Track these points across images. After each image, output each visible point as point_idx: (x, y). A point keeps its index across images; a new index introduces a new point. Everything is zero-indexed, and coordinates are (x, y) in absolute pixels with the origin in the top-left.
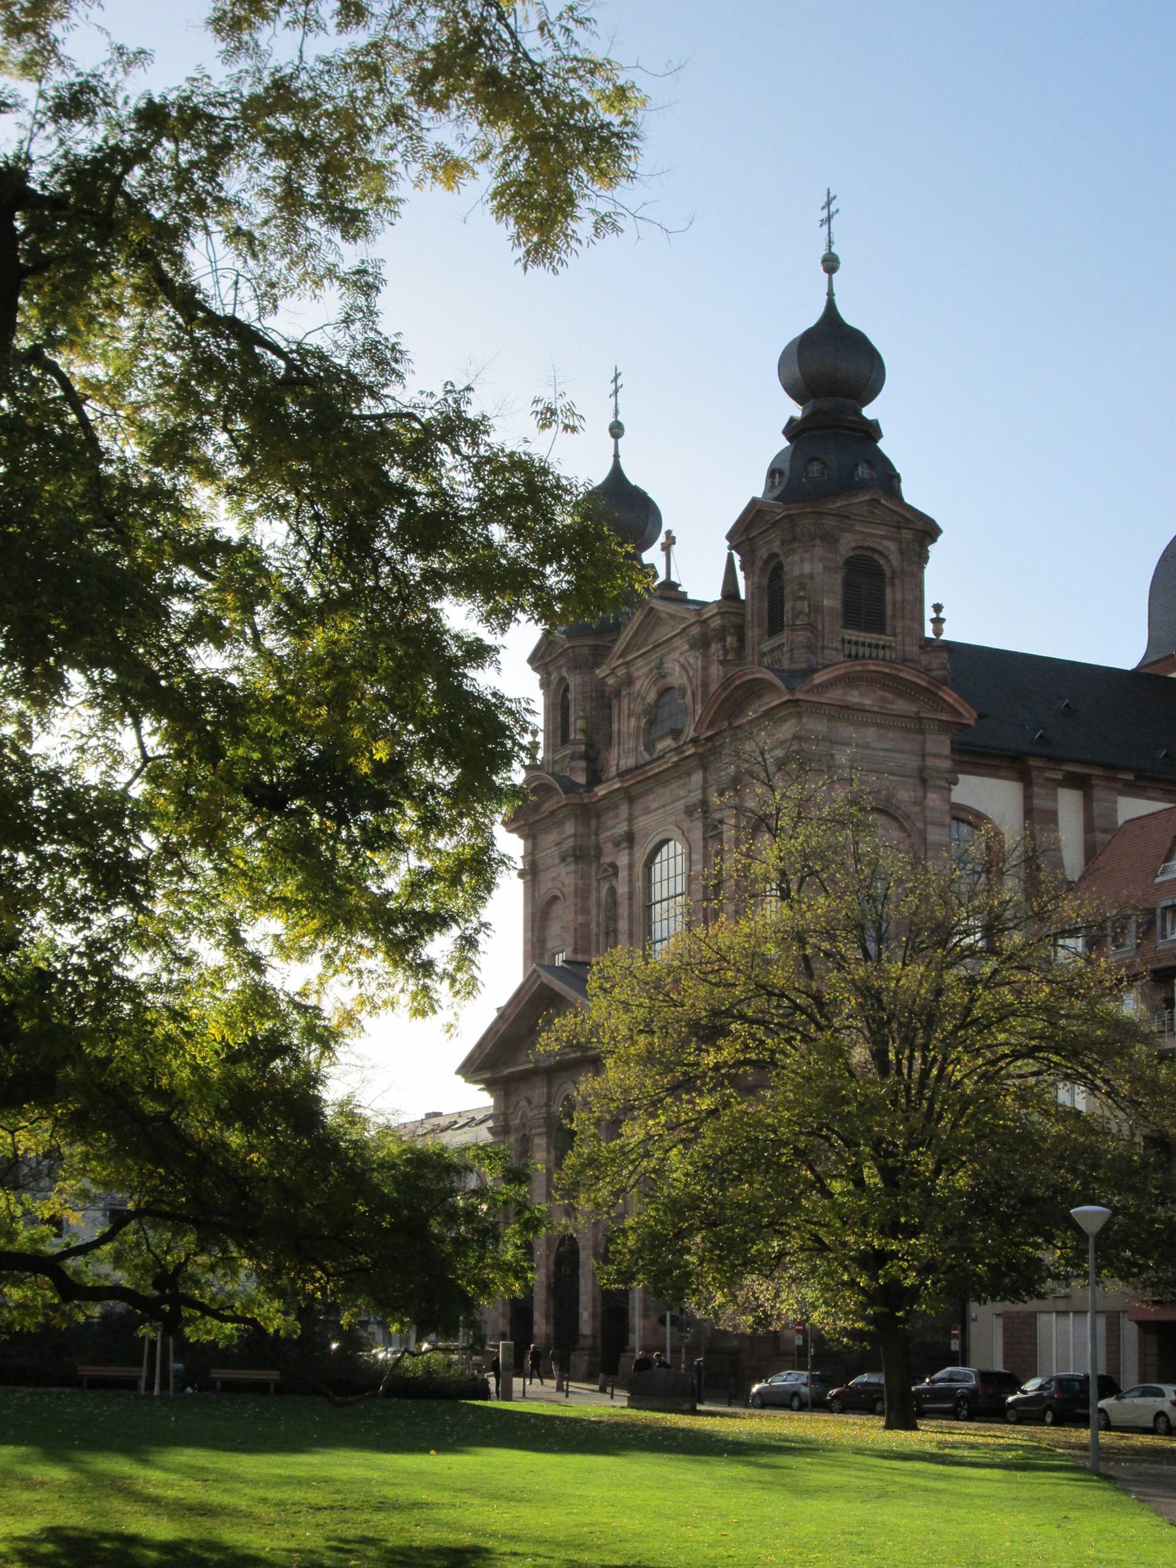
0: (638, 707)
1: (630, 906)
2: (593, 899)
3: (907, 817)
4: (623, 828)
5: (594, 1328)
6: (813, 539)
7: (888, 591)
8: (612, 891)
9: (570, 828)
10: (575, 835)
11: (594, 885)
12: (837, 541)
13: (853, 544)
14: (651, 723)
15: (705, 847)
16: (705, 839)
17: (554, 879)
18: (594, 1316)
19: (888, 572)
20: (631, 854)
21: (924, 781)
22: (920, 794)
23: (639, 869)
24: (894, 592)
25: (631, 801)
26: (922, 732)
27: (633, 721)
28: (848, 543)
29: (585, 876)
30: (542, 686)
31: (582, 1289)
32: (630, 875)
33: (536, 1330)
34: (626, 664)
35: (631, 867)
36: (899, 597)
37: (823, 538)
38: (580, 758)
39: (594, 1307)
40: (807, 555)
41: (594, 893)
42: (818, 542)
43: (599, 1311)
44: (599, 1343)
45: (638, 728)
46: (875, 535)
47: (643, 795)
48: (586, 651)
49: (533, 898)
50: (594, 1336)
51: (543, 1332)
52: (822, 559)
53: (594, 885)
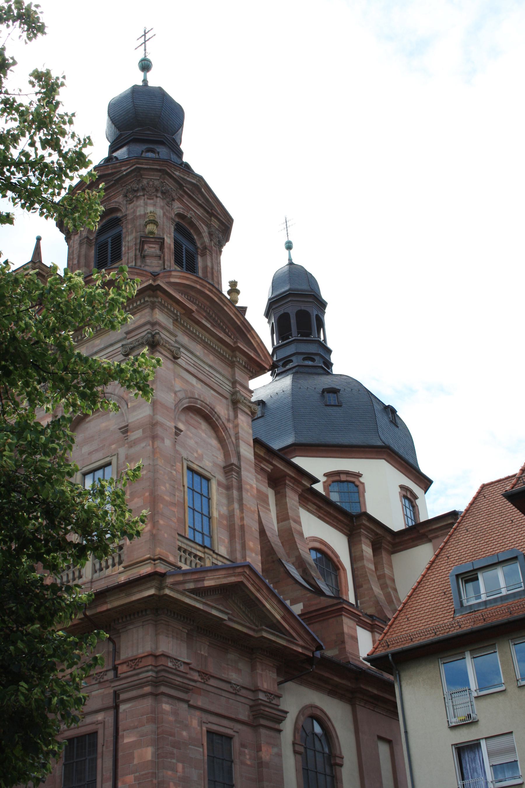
3: (225, 429)
6: (157, 191)
7: (200, 259)
13: (181, 211)
22: (231, 413)
24: (205, 261)
26: (232, 365)
37: (163, 193)
40: (150, 202)
42: (159, 194)
52: (162, 208)
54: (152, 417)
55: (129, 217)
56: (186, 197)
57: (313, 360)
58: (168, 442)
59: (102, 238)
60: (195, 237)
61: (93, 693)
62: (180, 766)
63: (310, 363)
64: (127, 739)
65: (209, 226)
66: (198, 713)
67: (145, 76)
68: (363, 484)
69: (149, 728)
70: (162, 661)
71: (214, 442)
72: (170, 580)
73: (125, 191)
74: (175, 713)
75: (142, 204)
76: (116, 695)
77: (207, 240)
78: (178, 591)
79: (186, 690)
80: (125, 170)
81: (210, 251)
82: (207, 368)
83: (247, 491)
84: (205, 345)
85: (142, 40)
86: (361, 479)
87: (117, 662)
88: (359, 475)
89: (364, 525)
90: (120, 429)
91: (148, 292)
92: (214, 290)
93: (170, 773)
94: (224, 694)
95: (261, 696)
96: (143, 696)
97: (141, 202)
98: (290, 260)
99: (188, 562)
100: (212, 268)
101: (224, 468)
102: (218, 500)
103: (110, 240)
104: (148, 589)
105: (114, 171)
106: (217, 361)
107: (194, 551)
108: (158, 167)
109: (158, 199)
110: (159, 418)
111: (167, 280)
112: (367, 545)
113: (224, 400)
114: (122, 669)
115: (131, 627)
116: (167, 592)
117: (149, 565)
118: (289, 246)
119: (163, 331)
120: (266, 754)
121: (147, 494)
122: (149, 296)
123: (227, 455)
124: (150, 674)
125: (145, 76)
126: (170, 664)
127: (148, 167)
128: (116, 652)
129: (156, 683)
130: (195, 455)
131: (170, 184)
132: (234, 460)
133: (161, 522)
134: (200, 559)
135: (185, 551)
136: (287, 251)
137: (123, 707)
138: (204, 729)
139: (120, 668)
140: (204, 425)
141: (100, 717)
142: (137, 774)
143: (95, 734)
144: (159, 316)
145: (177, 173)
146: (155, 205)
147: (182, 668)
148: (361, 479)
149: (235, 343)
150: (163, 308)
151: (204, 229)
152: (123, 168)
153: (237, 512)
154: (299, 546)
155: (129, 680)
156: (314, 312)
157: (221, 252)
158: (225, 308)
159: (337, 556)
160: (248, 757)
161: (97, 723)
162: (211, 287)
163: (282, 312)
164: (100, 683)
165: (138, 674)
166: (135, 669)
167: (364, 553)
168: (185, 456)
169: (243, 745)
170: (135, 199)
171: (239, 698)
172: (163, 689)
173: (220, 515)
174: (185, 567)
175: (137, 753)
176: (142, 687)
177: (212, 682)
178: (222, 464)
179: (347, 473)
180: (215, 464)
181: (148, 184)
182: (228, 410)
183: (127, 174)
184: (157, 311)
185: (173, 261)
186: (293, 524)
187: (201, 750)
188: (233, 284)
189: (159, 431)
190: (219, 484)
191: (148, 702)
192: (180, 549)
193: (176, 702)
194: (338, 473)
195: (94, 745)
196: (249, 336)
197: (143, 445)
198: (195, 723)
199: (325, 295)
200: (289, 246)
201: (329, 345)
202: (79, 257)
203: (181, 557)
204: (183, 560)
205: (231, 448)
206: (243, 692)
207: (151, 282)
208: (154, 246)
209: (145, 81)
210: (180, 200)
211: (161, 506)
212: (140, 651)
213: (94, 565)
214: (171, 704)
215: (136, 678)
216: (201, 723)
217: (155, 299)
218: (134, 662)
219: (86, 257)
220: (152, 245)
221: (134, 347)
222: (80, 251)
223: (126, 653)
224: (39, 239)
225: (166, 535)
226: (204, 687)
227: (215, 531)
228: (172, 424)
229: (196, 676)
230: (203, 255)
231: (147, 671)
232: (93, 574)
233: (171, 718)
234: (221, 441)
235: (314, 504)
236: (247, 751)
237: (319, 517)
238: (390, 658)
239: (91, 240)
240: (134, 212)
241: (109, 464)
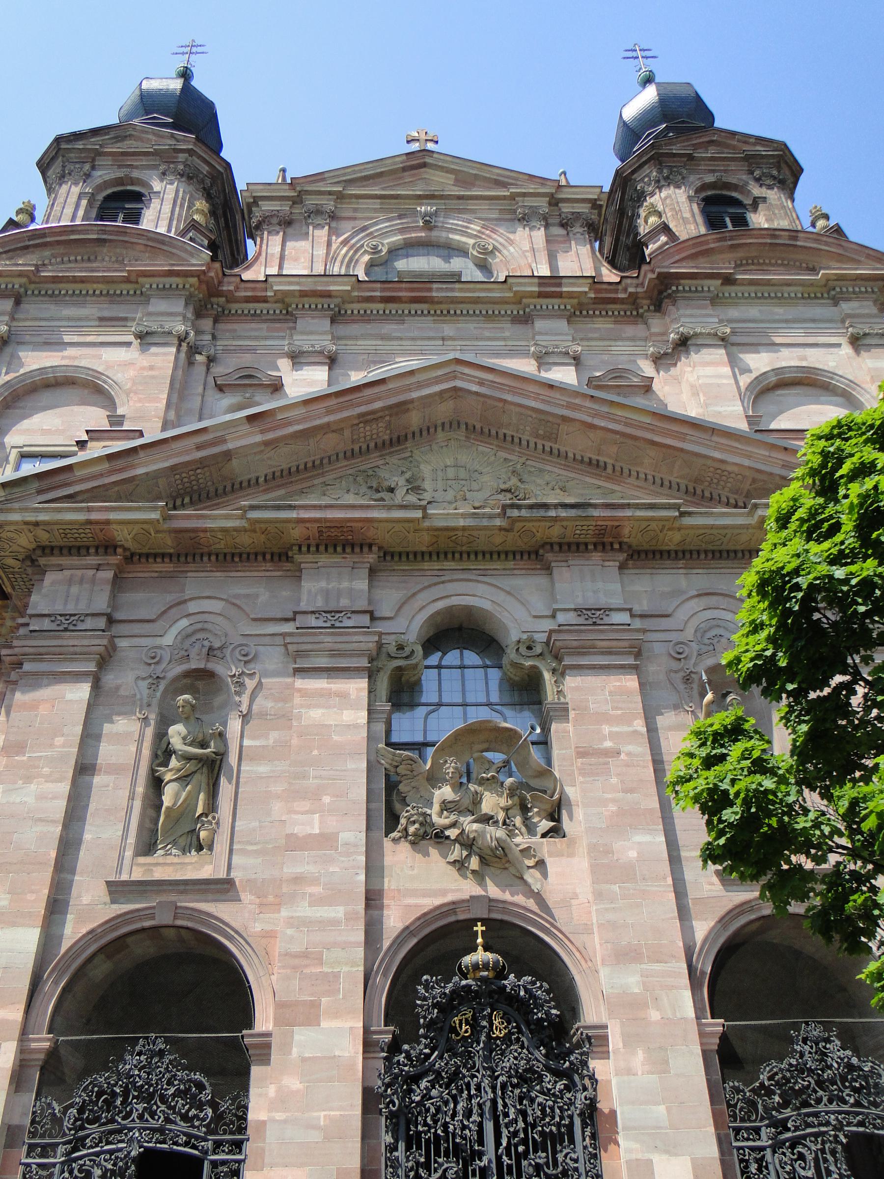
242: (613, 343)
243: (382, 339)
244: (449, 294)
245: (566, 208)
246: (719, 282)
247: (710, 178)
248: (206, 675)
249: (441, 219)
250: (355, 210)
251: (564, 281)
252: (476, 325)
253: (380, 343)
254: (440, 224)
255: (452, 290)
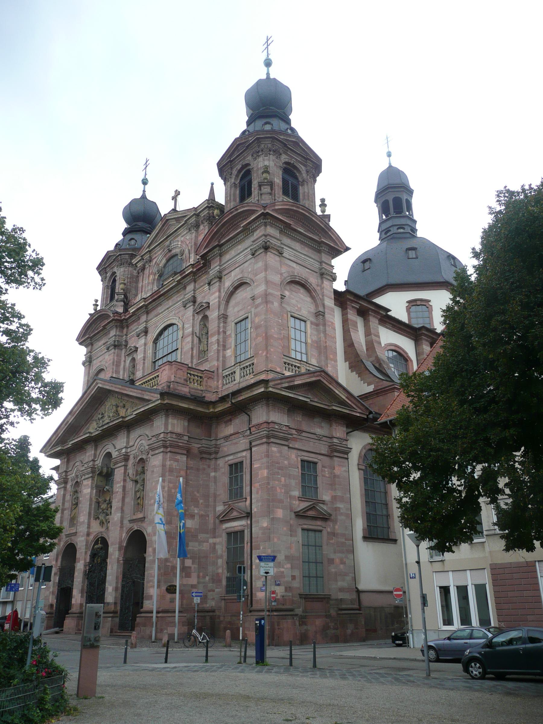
0: (155, 270)
1: (144, 363)
2: (122, 366)
3: (315, 291)
4: (142, 327)
5: (116, 598)
6: (270, 151)
7: (300, 187)
8: (133, 360)
9: (113, 333)
10: (115, 335)
11: (123, 359)
12: (281, 154)
13: (287, 160)
14: (160, 276)
15: (193, 320)
16: (193, 316)
17: (100, 362)
18: (116, 589)
19: (300, 179)
20: (146, 338)
21: (322, 275)
22: (320, 281)
23: (150, 345)
25: (148, 313)
26: (319, 251)
27: (151, 277)
28: (284, 158)
29: (119, 356)
30: (102, 281)
31: (109, 571)
32: (145, 348)
33: (73, 601)
34: (150, 251)
35: (145, 344)
36: (306, 190)
37: (274, 151)
38: (121, 301)
39: (117, 583)
41: (122, 363)
43: (120, 585)
44: (119, 608)
45: (154, 279)
46: (296, 160)
47: (154, 309)
48: (127, 256)
49: (89, 373)
50: (115, 603)
51: (79, 602)
52: (273, 161)
53: (123, 359)
54: (266, 290)
55: (255, 169)
56: (289, 150)
57: (404, 228)
58: (276, 304)
59: (243, 183)
60: (298, 174)
61: (241, 442)
62: (283, 479)
63: (402, 231)
64: (256, 466)
65: (305, 166)
66: (295, 451)
67: (268, 70)
68: (431, 306)
69: (265, 460)
70: (271, 425)
71: (309, 299)
72: (271, 384)
73: (252, 153)
74: (280, 452)
75: (262, 160)
76: (251, 443)
77: (304, 175)
78: (277, 389)
79: (286, 439)
80: (251, 140)
81: (307, 182)
82: (303, 256)
83: (329, 326)
84: (302, 243)
85: (266, 46)
86: (430, 303)
87: (250, 426)
88: (429, 301)
89: (424, 334)
90: (251, 298)
91: (262, 217)
92: (305, 209)
93: (277, 482)
94: (312, 440)
95: (335, 440)
96: (262, 444)
97: (261, 159)
98: (390, 164)
99: (291, 370)
100: (308, 193)
101: (316, 313)
102: (311, 333)
103: (246, 183)
104: (260, 388)
105: (245, 140)
106: (310, 251)
107: (294, 364)
108: (270, 136)
109: (271, 155)
110: (270, 291)
111: (273, 208)
112: (427, 345)
113: (315, 274)
114: (253, 429)
115: (256, 407)
116: (271, 389)
117: (264, 374)
118: (389, 155)
119: (272, 239)
120: (337, 471)
121: (264, 335)
122: (263, 219)
123: (317, 306)
124: (265, 432)
125: (268, 70)
126: (276, 427)
127: (264, 136)
128: (250, 421)
129: (268, 437)
130: (296, 308)
131: (278, 145)
132: (321, 309)
133: (272, 350)
134: (299, 367)
135: (288, 364)
136: (388, 158)
137: (253, 449)
138: (299, 459)
139: (251, 428)
140: (302, 290)
141: (244, 454)
142: (260, 483)
143: (242, 463)
144: (270, 230)
145: (282, 137)
146: (269, 160)
147: (284, 429)
148: (430, 303)
149: (320, 239)
150: (272, 225)
151: (302, 168)
152: (250, 139)
153: (323, 339)
154: (377, 350)
155: (256, 435)
156: (404, 197)
157: (315, 181)
158: (313, 218)
159: (406, 353)
160: (327, 473)
161: (243, 457)
162: (303, 208)
163: (384, 200)
164: (244, 436)
165: (259, 432)
166: (258, 430)
167: (424, 350)
168: (289, 309)
169: (323, 467)
170: (257, 157)
171: (321, 442)
172: (272, 440)
173: (312, 341)
174: (287, 374)
175: (260, 472)
176: (262, 439)
177: (304, 434)
178: (315, 312)
179: (421, 300)
180: (309, 312)
181: (264, 147)
182: (317, 279)
183: (252, 142)
184: (268, 227)
185: (281, 193)
186: (374, 338)
187: (297, 470)
188: (323, 200)
189: (270, 298)
190: (312, 323)
191: (264, 447)
192: (285, 363)
193: (281, 446)
194: (415, 300)
195: (242, 467)
196: (330, 233)
197: (262, 307)
198: (293, 456)
199: (412, 185)
200: (389, 155)
201: (415, 217)
202: (230, 195)
203: (286, 367)
204: (287, 369)
205: (319, 302)
206: (324, 439)
207: (263, 211)
208: (266, 187)
209: (268, 74)
210: (286, 153)
211: (272, 341)
212: (261, 420)
213: (240, 374)
214: (277, 448)
215: (258, 434)
216: (297, 456)
217: (266, 221)
218: (258, 425)
219: (235, 195)
220: (265, 187)
221: (257, 250)
222: (230, 192)
223: (254, 422)
224: (212, 184)
225: (275, 357)
226: (299, 437)
227: (309, 351)
228: (279, 293)
229: (294, 432)
230: (303, 185)
231: (264, 431)
232: (240, 379)
233: (278, 455)
234: (312, 297)
235: (391, 324)
236: (326, 469)
237: (394, 331)
238: (388, 423)
239: (236, 184)
240: (258, 165)
241: (247, 317)
242: (203, 287)
243: (156, 316)
244: (164, 291)
245: (202, 215)
246: (218, 248)
247: (239, 167)
248: (77, 482)
249: (172, 245)
250: (155, 254)
251: (185, 270)
252: (176, 296)
253: (155, 318)
254: (173, 247)
255: (164, 289)
